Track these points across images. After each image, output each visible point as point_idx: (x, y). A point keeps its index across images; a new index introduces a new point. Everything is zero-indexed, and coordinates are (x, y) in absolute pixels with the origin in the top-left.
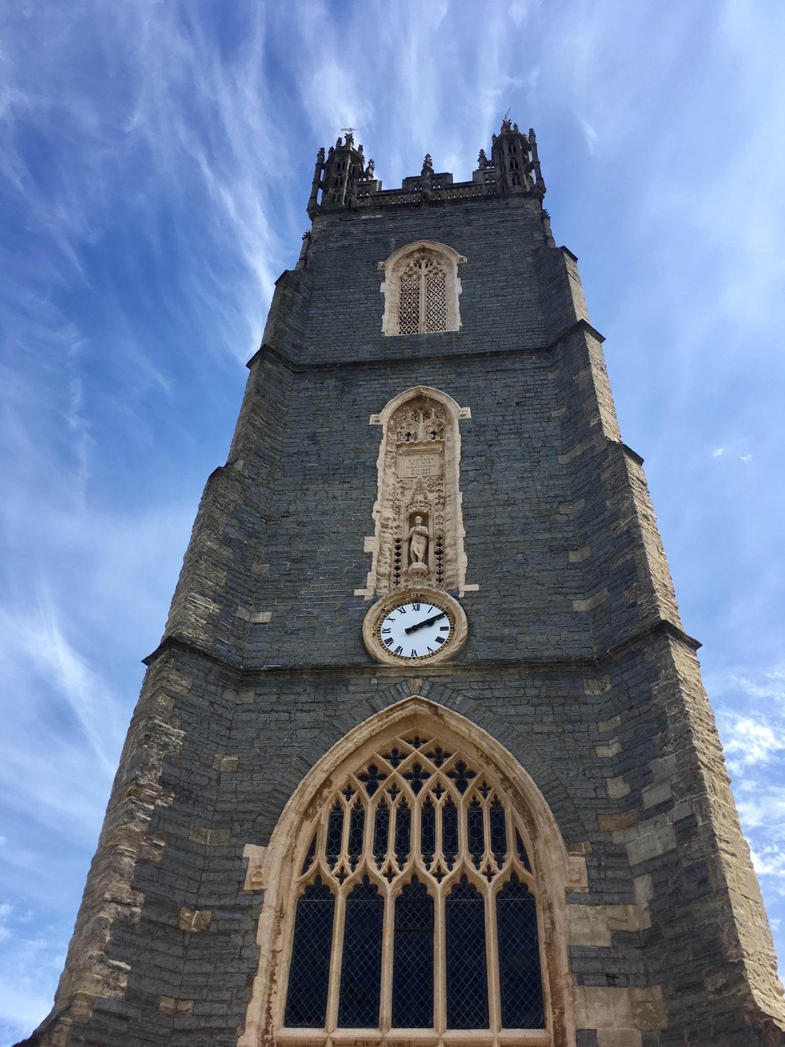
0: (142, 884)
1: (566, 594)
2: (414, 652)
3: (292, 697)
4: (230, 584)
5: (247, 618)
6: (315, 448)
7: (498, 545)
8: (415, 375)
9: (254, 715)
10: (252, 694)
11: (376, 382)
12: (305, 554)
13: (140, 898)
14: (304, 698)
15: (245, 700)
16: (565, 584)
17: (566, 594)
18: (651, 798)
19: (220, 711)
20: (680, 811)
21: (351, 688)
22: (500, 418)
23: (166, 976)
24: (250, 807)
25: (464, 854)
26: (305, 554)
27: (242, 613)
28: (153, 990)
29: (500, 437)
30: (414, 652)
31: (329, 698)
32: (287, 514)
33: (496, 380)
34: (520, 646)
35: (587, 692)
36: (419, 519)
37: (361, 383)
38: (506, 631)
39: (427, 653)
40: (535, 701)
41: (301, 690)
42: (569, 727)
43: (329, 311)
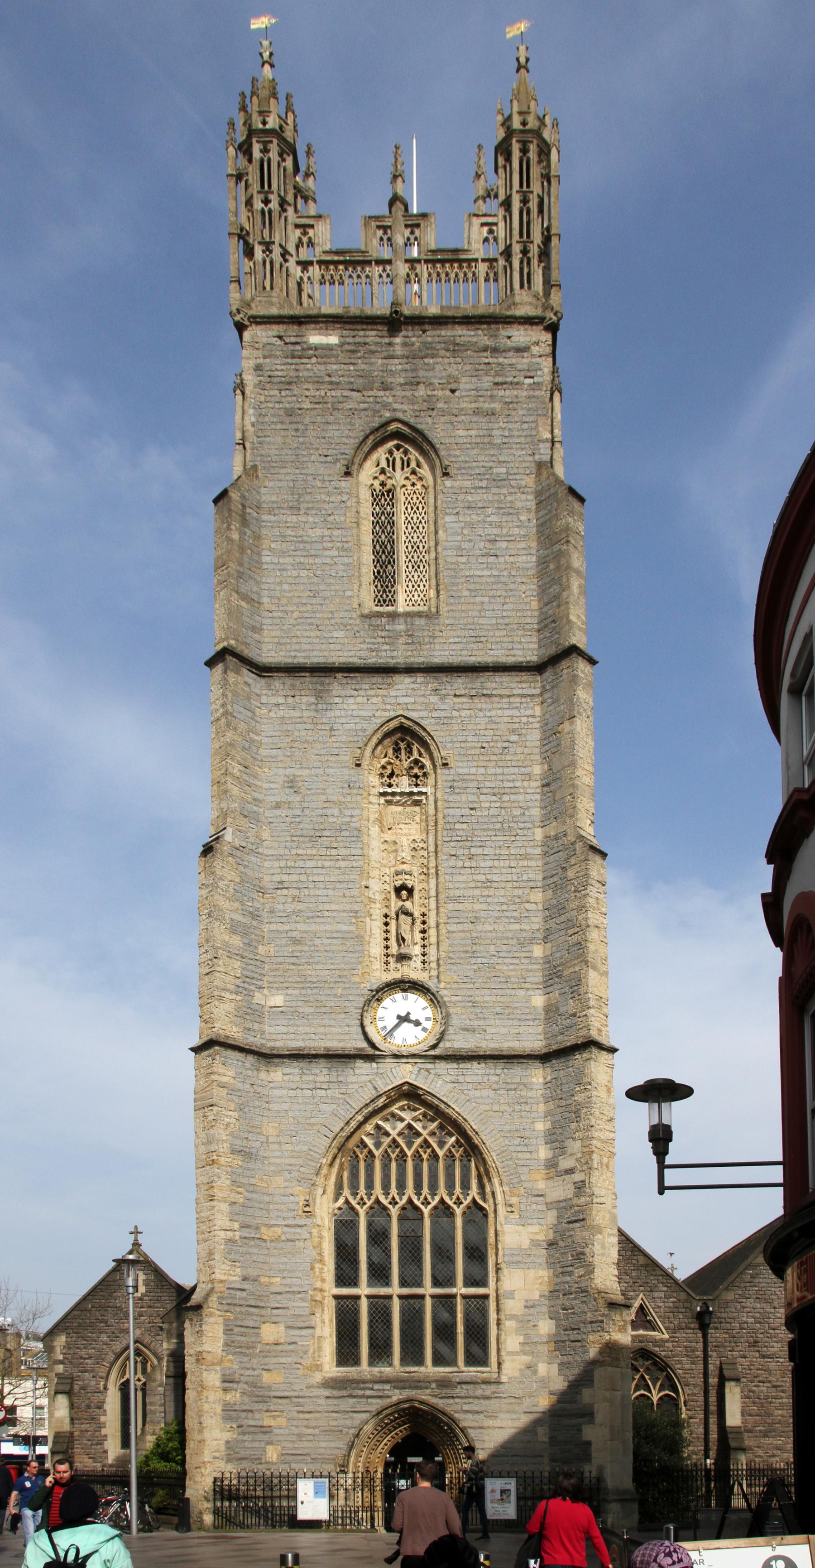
0: (236, 1218)
1: (528, 989)
2: (404, 1040)
3: (311, 1078)
4: (245, 973)
5: (263, 1003)
6: (298, 798)
7: (474, 935)
8: (393, 693)
9: (285, 1092)
10: (279, 1073)
11: (351, 700)
12: (305, 935)
13: (236, 1226)
14: (321, 1078)
15: (276, 1079)
16: (528, 980)
17: (528, 989)
18: (565, 1163)
19: (259, 1089)
20: (578, 1177)
21: (357, 1071)
22: (482, 770)
23: (261, 1266)
24: (293, 1161)
25: (442, 1192)
26: (305, 935)
27: (258, 998)
28: (255, 1274)
29: (483, 797)
30: (404, 1040)
31: (340, 1079)
32: (281, 886)
33: (481, 710)
34: (487, 1037)
35: (534, 1080)
36: (404, 893)
37: (337, 700)
38: (476, 1023)
39: (415, 1041)
40: (495, 1086)
41: (318, 1071)
42: (517, 1108)
43: (288, 560)
